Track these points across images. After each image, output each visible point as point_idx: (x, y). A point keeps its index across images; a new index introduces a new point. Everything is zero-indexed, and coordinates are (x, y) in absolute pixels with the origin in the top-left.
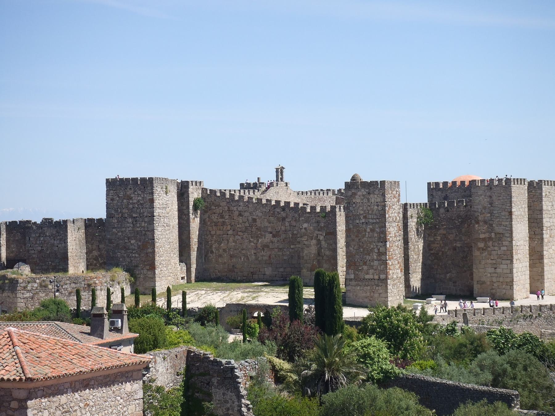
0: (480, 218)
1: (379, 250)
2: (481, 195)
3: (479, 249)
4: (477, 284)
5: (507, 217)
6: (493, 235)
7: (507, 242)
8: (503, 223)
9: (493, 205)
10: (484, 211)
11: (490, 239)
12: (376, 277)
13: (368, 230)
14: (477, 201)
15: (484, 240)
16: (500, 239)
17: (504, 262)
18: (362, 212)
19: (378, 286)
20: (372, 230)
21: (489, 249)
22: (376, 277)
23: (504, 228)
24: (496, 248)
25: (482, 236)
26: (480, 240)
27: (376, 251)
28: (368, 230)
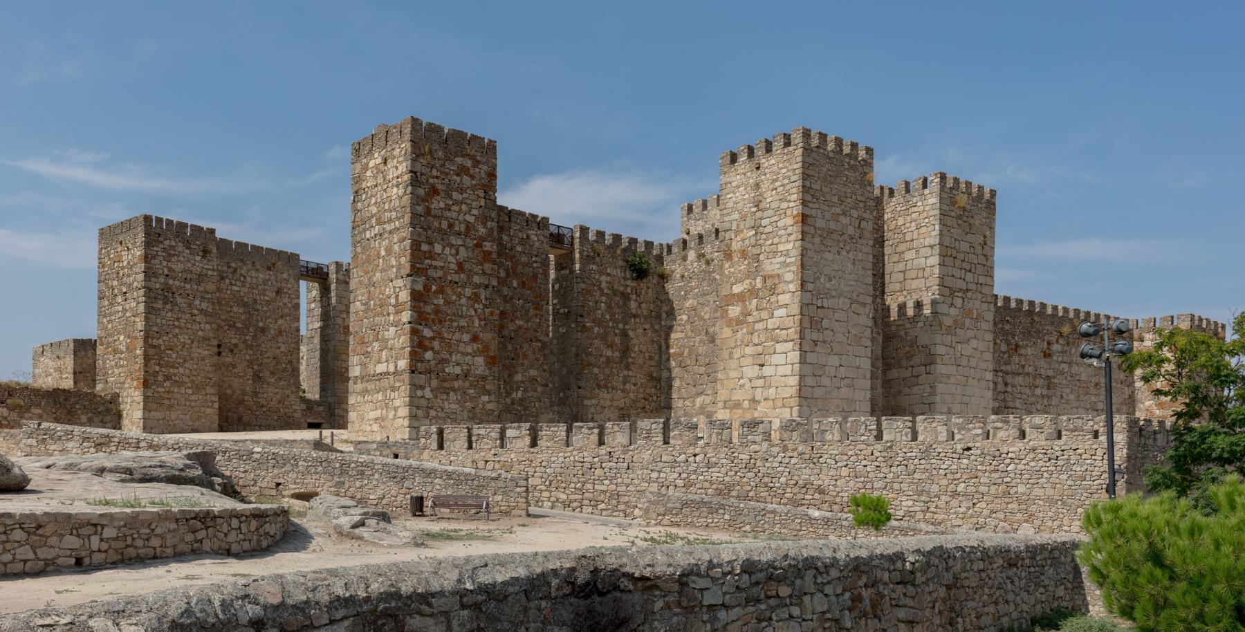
0: (735, 246)
1: (397, 296)
2: (738, 187)
3: (730, 323)
4: (725, 408)
5: (790, 230)
6: (759, 283)
7: (788, 296)
8: (781, 247)
9: (762, 205)
10: (742, 227)
11: (753, 292)
12: (392, 369)
13: (383, 253)
14: (730, 205)
15: (741, 298)
16: (773, 291)
17: (779, 347)
18: (374, 210)
19: (393, 389)
20: (389, 250)
21: (750, 319)
22: (392, 369)
23: (782, 259)
24: (764, 315)
25: (737, 289)
26: (732, 299)
27: (393, 301)
28: (383, 253)
